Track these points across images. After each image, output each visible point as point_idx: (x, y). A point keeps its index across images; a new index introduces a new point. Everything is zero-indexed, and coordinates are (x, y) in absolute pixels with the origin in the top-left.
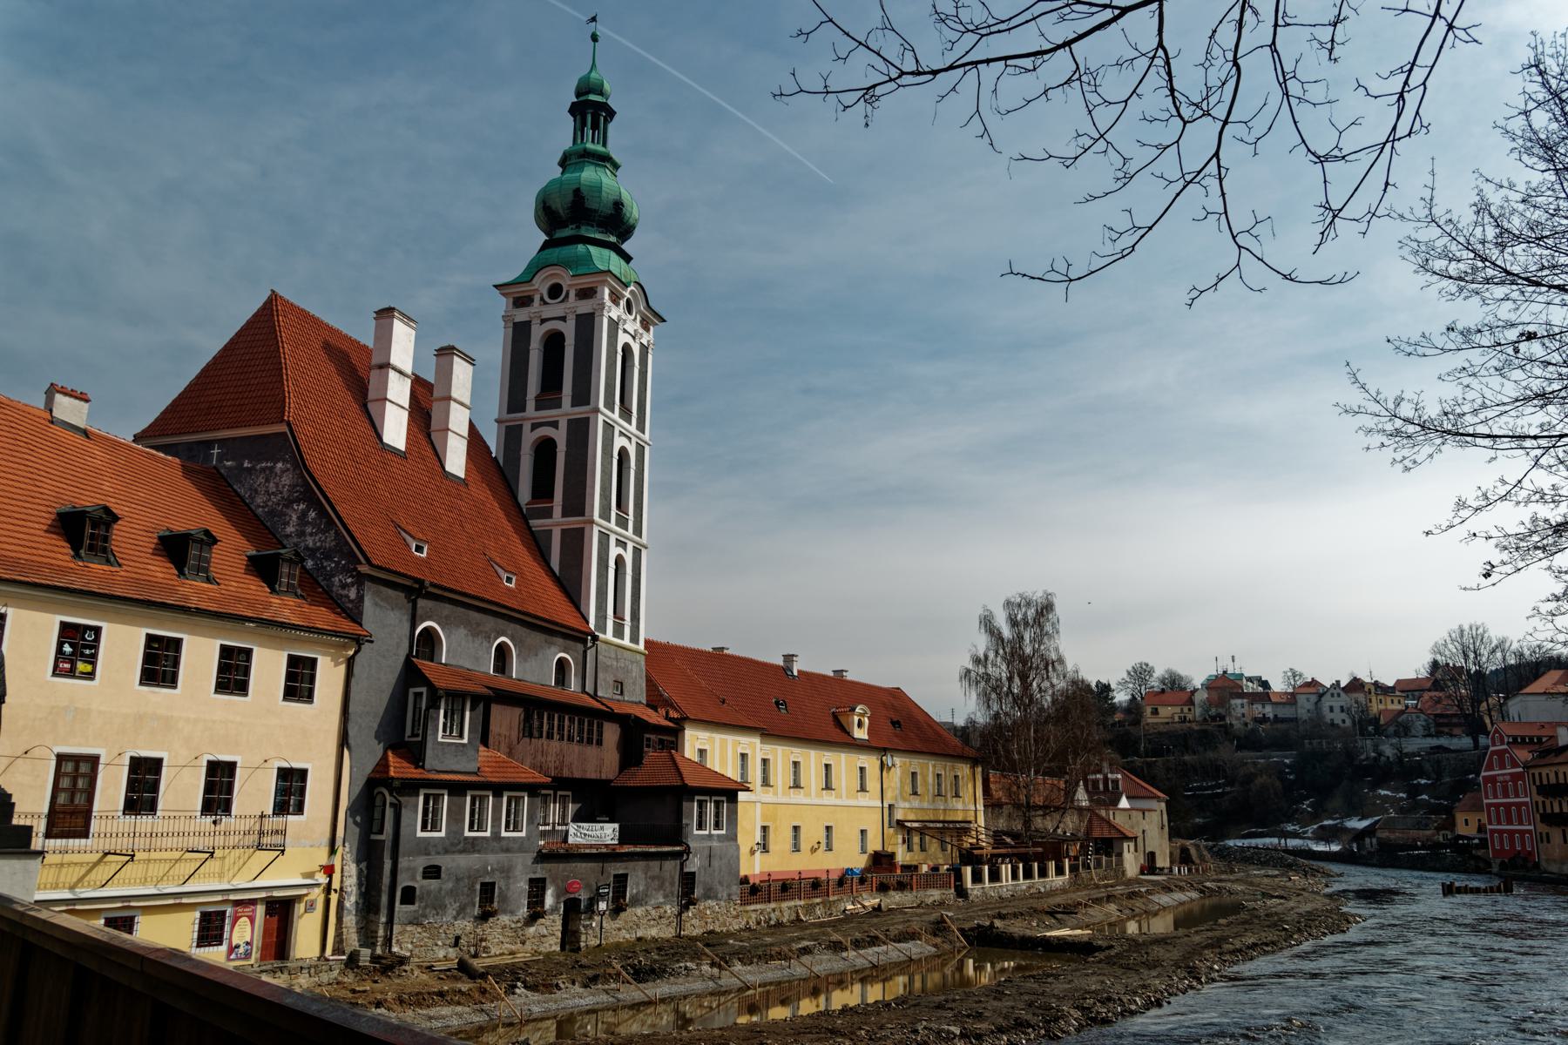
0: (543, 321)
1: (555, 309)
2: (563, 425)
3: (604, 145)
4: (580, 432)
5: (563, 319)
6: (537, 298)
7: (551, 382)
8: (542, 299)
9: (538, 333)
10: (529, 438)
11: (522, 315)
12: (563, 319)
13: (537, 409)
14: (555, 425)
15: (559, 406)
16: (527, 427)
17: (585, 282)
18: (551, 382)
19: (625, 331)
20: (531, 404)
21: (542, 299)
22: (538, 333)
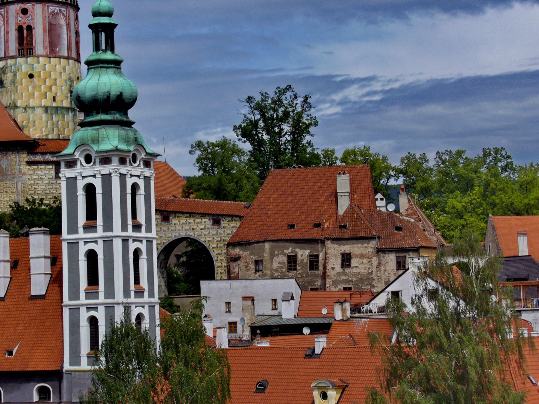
0: (84, 177)
2: (100, 242)
3: (112, 50)
5: (94, 176)
6: (79, 163)
7: (91, 214)
8: (81, 164)
9: (81, 184)
10: (83, 249)
13: (85, 232)
15: (96, 232)
16: (81, 243)
18: (91, 214)
19: (132, 176)
20: (81, 230)
21: (81, 164)
22: (81, 184)
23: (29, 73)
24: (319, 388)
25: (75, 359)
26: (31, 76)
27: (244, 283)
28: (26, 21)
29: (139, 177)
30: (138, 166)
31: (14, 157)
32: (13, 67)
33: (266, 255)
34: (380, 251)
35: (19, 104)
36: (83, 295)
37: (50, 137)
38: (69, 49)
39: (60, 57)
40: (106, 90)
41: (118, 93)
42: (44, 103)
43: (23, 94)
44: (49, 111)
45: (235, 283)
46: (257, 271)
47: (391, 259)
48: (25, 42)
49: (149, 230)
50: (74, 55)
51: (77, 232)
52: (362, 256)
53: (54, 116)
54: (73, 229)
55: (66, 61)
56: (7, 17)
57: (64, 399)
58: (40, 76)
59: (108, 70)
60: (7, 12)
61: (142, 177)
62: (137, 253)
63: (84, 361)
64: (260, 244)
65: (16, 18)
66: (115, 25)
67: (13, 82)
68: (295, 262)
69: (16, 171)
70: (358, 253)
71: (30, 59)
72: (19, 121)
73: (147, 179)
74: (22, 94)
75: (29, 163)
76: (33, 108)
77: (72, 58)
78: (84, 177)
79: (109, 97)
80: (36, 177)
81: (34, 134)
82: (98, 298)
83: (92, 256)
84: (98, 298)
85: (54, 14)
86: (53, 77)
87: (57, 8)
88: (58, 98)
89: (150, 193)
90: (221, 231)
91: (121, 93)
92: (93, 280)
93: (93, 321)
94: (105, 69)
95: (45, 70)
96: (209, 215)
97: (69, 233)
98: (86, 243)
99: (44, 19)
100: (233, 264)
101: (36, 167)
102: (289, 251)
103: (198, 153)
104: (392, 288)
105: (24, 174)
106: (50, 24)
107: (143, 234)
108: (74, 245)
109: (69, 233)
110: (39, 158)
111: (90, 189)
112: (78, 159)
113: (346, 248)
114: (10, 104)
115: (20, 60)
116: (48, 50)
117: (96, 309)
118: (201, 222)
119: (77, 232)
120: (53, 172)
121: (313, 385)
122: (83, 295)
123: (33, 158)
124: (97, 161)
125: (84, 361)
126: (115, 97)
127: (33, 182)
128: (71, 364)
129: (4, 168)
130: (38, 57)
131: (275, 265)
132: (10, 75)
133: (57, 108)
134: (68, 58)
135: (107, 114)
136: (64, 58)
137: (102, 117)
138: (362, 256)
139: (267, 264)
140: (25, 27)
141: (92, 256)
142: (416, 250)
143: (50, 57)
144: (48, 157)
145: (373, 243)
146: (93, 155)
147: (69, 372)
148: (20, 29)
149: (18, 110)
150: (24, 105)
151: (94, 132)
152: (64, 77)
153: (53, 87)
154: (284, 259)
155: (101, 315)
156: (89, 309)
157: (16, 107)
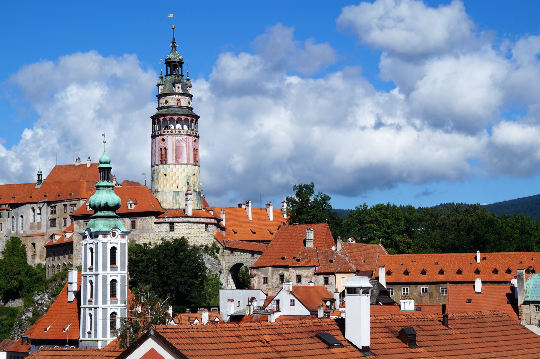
12: (92, 244)
19: (111, 243)
26: (165, 175)
29: (117, 243)
33: (270, 274)
34: (316, 274)
37: (174, 208)
38: (188, 159)
39: (182, 164)
42: (171, 189)
46: (264, 283)
47: (321, 278)
48: (164, 156)
49: (123, 269)
50: (192, 161)
52: (307, 277)
61: (119, 243)
62: (114, 282)
64: (267, 268)
65: (159, 144)
66: (111, 168)
67: (157, 178)
68: (283, 279)
69: (150, 227)
70: (305, 275)
73: (123, 245)
75: (156, 223)
77: (189, 164)
79: (100, 205)
81: (165, 206)
82: (117, 303)
84: (117, 303)
85: (179, 141)
86: (177, 175)
87: (181, 138)
99: (173, 144)
102: (281, 272)
104: (276, 298)
105: (153, 229)
106: (176, 146)
107: (119, 271)
110: (161, 220)
113: (299, 272)
116: (175, 161)
120: (168, 228)
123: (158, 220)
129: (144, 225)
131: (274, 280)
132: (156, 174)
133: (178, 192)
134: (187, 164)
136: (185, 164)
137: (99, 214)
138: (307, 277)
139: (269, 279)
142: (334, 274)
145: (312, 270)
148: (161, 149)
152: (184, 174)
153: (177, 181)
154: (278, 277)
157: (158, 192)
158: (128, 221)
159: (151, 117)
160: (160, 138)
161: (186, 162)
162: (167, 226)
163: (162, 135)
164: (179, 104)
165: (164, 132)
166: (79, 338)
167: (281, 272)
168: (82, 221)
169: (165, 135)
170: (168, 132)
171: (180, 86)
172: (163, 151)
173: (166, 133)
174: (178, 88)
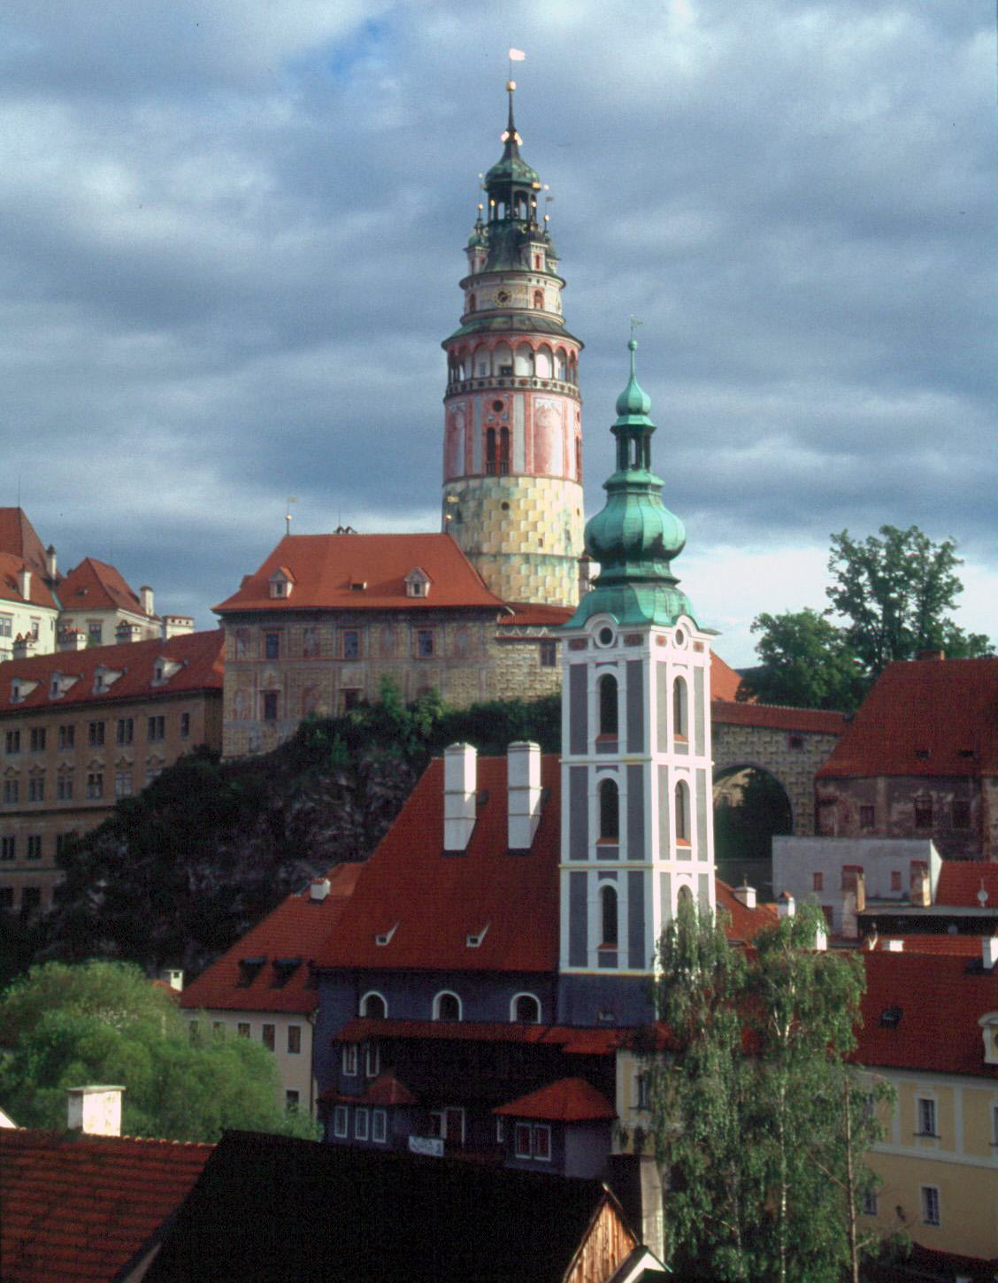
0: (598, 665)
1: (606, 653)
4: (637, 775)
5: (615, 664)
6: (590, 643)
8: (595, 644)
9: (593, 676)
11: (578, 658)
14: (615, 768)
17: (631, 630)
21: (595, 644)
22: (593, 676)
23: (502, 501)
24: (992, 1027)
25: (579, 957)
26: (506, 506)
27: (845, 842)
28: (500, 422)
30: (686, 649)
31: (474, 629)
32: (478, 492)
35: (485, 548)
36: (592, 852)
37: (533, 600)
39: (551, 478)
40: (637, 530)
41: (656, 535)
42: (524, 548)
43: (493, 534)
44: (532, 560)
45: (829, 844)
48: (498, 452)
50: (572, 474)
51: (584, 751)
53: (539, 569)
54: (579, 746)
55: (560, 482)
56: (471, 413)
57: (561, 1018)
58: (518, 507)
59: (640, 498)
60: (471, 407)
63: (593, 958)
67: (478, 514)
71: (503, 481)
72: (485, 573)
73: (699, 671)
74: (490, 533)
76: (507, 556)
78: (598, 665)
80: (510, 663)
83: (608, 789)
88: (546, 543)
89: (702, 693)
90: (803, 758)
91: (661, 536)
92: (609, 828)
93: (609, 896)
94: (634, 497)
95: (526, 497)
96: (784, 730)
97: (574, 751)
98: (599, 768)
100: (823, 811)
101: (510, 647)
103: (762, 633)
108: (579, 774)
109: (574, 751)
110: (515, 632)
111: (608, 684)
112: (590, 635)
114: (471, 549)
115: (489, 481)
117: (613, 875)
118: (771, 742)
119: (584, 751)
120: (537, 656)
121: (982, 1021)
122: (592, 852)
124: (621, 640)
125: (593, 958)
126: (651, 541)
127: (504, 670)
128: (572, 963)
130: (517, 477)
132: (472, 504)
133: (544, 556)
134: (564, 479)
135: (638, 566)
136: (557, 478)
140: (498, 429)
141: (608, 789)
143: (535, 478)
144: (530, 632)
146: (615, 630)
147: (568, 976)
148: (490, 432)
149: (484, 559)
150: (493, 551)
151: (616, 595)
153: (540, 525)
155: (621, 887)
156: (602, 875)
158: (406, 635)
159: (445, 345)
160: (493, 397)
161: (561, 475)
162: (532, 652)
163: (494, 390)
164: (538, 305)
165: (501, 383)
166: (557, 967)
167: (920, 793)
168: (254, 629)
169: (505, 390)
170: (513, 382)
171: (542, 253)
172: (498, 440)
173: (508, 384)
174: (538, 258)
